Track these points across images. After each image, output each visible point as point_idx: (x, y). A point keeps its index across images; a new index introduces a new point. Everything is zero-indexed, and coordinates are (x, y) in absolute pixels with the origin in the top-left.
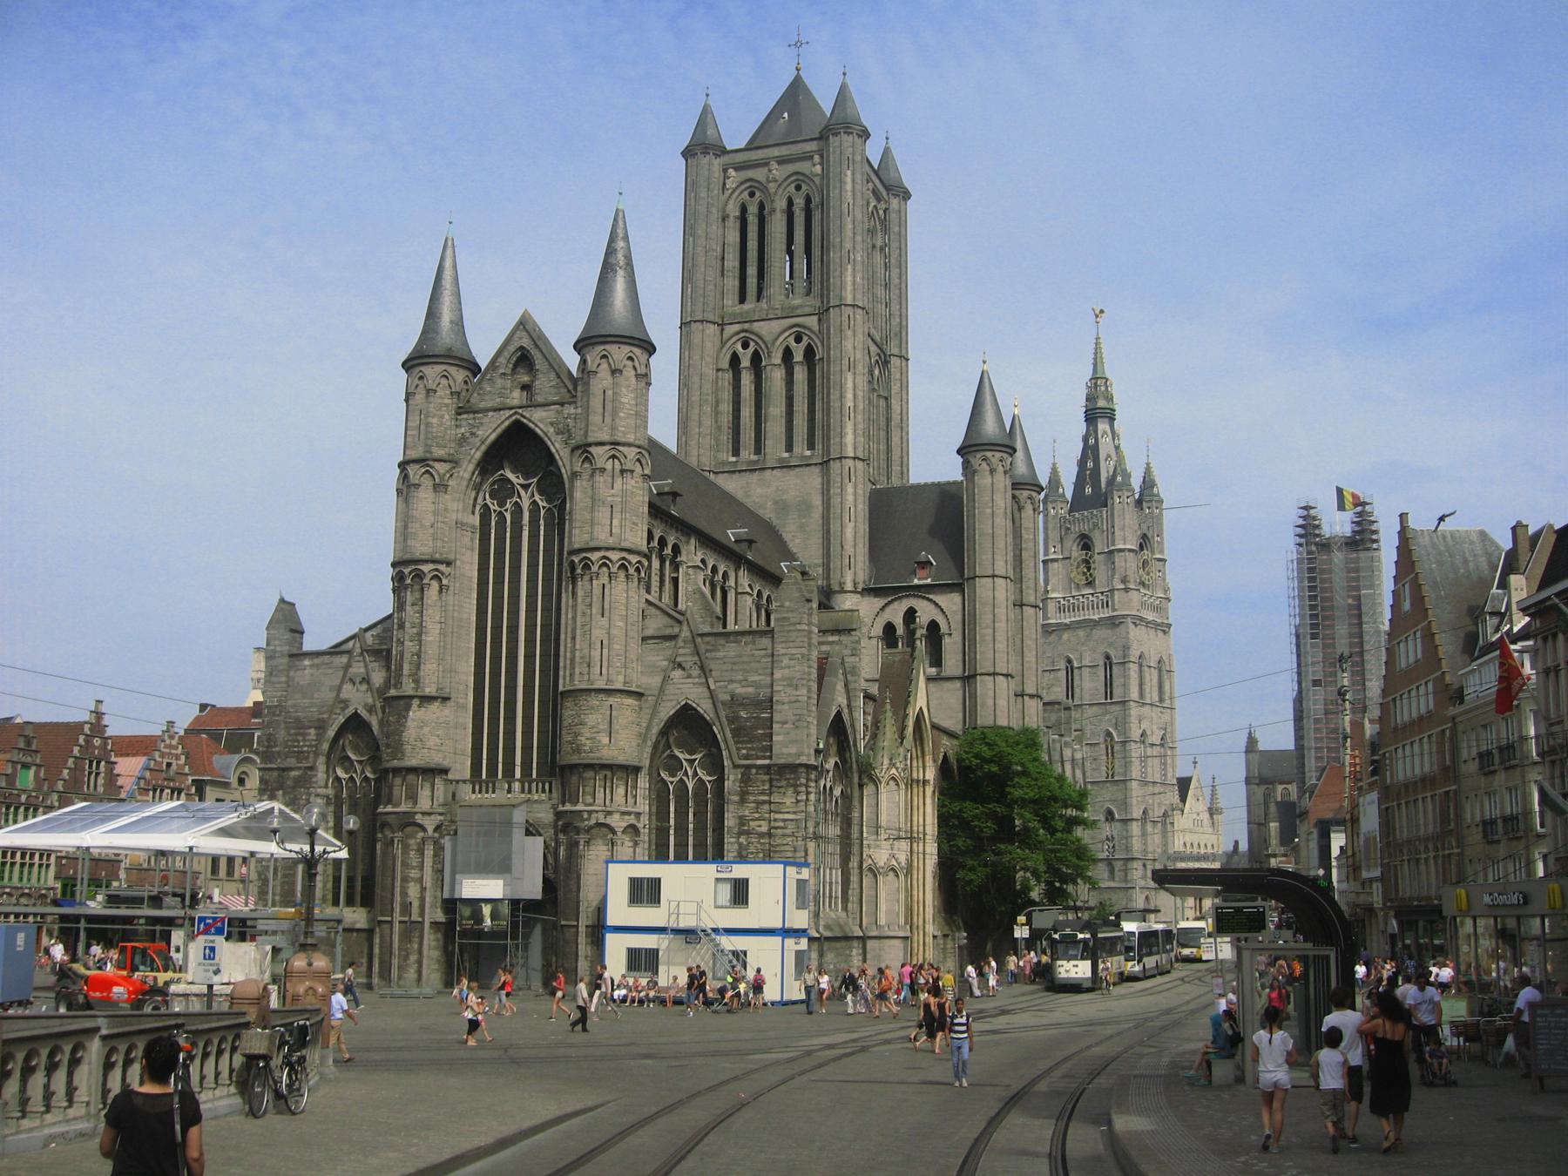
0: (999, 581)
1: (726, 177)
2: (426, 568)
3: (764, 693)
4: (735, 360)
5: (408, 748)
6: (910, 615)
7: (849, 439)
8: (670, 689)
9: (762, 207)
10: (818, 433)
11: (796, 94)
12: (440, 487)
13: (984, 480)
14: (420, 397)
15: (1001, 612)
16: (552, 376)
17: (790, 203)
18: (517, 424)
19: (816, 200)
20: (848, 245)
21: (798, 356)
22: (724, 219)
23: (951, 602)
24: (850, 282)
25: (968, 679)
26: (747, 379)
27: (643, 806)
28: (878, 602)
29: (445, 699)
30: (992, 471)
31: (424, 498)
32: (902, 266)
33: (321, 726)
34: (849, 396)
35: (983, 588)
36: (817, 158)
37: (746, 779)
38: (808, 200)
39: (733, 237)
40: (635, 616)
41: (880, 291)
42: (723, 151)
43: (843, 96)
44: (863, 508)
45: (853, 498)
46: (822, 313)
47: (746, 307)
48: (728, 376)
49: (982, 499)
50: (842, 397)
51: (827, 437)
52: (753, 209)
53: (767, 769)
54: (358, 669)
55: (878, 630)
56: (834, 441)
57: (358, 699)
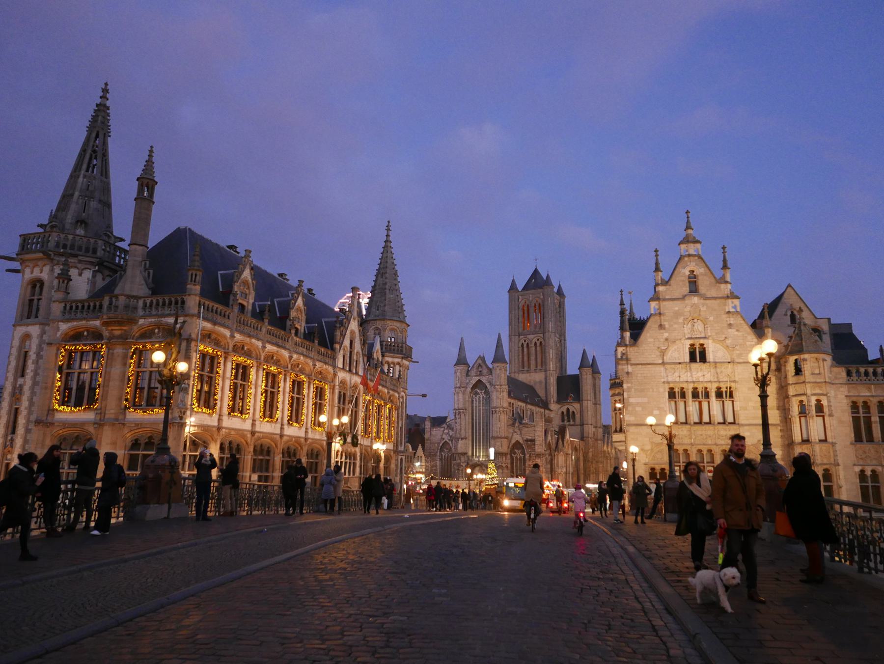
0: (589, 402)
1: (519, 298)
2: (461, 411)
3: (533, 438)
4: (522, 345)
5: (459, 449)
6: (568, 409)
7: (551, 366)
8: (514, 437)
9: (528, 306)
10: (543, 364)
11: (536, 272)
12: (464, 393)
13: (584, 377)
14: (458, 374)
15: (589, 409)
16: (487, 370)
17: (535, 305)
18: (479, 380)
19: (541, 303)
20: (550, 317)
21: (538, 344)
22: (519, 308)
23: (577, 406)
24: (550, 326)
25: (582, 425)
26: (525, 349)
27: (509, 461)
28: (559, 406)
29: (466, 439)
30: (587, 374)
31: (461, 395)
32: (564, 316)
33: (439, 444)
34: (551, 355)
35: (585, 403)
36: (541, 294)
37: (530, 456)
38: (540, 304)
39: (521, 313)
40: (506, 422)
41: (559, 324)
42: (518, 291)
43: (548, 276)
44: (555, 383)
45: (553, 381)
46: (544, 333)
47: (525, 331)
48: (521, 348)
49: (584, 381)
50: (549, 355)
51: (546, 365)
52: (526, 306)
53: (534, 454)
54: (446, 431)
55: (560, 413)
56: (548, 366)
57: (446, 438)
